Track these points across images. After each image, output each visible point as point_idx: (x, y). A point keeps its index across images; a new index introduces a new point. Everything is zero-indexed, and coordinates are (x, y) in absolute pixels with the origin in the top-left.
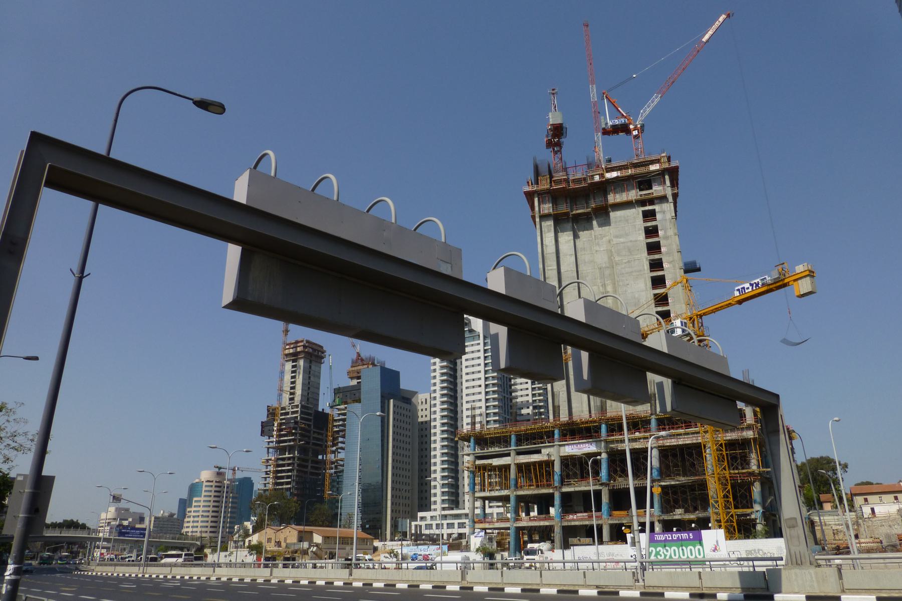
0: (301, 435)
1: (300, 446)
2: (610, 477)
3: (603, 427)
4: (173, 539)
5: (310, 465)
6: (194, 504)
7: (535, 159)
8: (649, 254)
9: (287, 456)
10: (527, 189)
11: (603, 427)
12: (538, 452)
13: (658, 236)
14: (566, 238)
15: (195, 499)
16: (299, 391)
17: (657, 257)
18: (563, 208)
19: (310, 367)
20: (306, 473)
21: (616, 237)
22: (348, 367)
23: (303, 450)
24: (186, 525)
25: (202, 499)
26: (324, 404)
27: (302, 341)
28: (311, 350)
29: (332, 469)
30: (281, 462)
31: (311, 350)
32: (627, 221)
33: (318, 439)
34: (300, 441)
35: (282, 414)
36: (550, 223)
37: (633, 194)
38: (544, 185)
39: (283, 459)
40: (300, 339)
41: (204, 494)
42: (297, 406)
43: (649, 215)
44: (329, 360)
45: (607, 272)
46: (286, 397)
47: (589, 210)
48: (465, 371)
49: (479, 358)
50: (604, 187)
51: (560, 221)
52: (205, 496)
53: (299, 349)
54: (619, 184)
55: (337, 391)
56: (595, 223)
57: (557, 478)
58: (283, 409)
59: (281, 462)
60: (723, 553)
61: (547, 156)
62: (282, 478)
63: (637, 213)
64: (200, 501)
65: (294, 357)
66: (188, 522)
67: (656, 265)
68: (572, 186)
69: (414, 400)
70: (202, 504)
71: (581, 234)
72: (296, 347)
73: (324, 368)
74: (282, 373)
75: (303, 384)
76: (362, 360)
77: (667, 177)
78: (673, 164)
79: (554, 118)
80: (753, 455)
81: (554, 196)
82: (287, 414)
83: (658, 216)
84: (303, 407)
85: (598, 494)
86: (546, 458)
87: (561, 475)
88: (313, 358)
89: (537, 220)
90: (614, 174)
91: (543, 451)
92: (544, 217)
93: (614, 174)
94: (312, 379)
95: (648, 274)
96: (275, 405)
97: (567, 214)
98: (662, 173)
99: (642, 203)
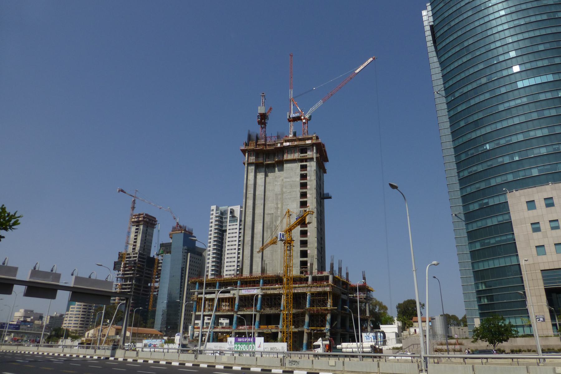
0: (138, 271)
1: (136, 278)
2: (261, 308)
3: (261, 281)
4: (25, 330)
5: (142, 289)
6: (71, 309)
7: (249, 131)
8: (301, 189)
9: (128, 283)
10: (243, 148)
11: (261, 281)
12: (228, 292)
13: (306, 179)
14: (261, 176)
15: (71, 306)
16: (138, 244)
17: (304, 190)
18: (261, 160)
19: (147, 230)
20: (139, 294)
21: (286, 178)
22: (170, 230)
23: (138, 280)
24: (65, 322)
25: (76, 306)
26: (153, 253)
27: (143, 214)
28: (148, 220)
29: (155, 292)
30: (124, 287)
31: (148, 220)
32: (292, 169)
33: (149, 274)
34: (137, 274)
35: (127, 258)
36: (252, 168)
37: (297, 156)
38: (252, 147)
39: (126, 285)
40: (141, 213)
42: (137, 253)
43: (304, 168)
44: (158, 227)
45: (279, 197)
46: (130, 248)
47: (274, 162)
48: (228, 240)
49: (236, 233)
50: (283, 150)
51: (258, 167)
53: (140, 219)
54: (290, 149)
55: (162, 245)
56: (276, 169)
57: (236, 307)
58: (129, 254)
59: (124, 287)
60: (261, 349)
61: (257, 130)
63: (298, 165)
64: (74, 308)
65: (137, 223)
67: (304, 195)
68: (268, 148)
69: (204, 254)
71: (269, 174)
72: (139, 218)
73: (155, 230)
74: (129, 233)
75: (141, 240)
76: (180, 227)
77: (315, 148)
78: (320, 141)
79: (261, 110)
80: (329, 300)
81: (257, 153)
82: (130, 257)
83: (308, 169)
84: (140, 254)
85: (255, 315)
86: (232, 296)
87: (238, 305)
89: (246, 165)
90: (288, 144)
91: (231, 292)
92: (249, 164)
93: (288, 144)
94: (147, 237)
95: (299, 200)
96: (124, 252)
97: (262, 163)
98: (312, 145)
99: (301, 160)
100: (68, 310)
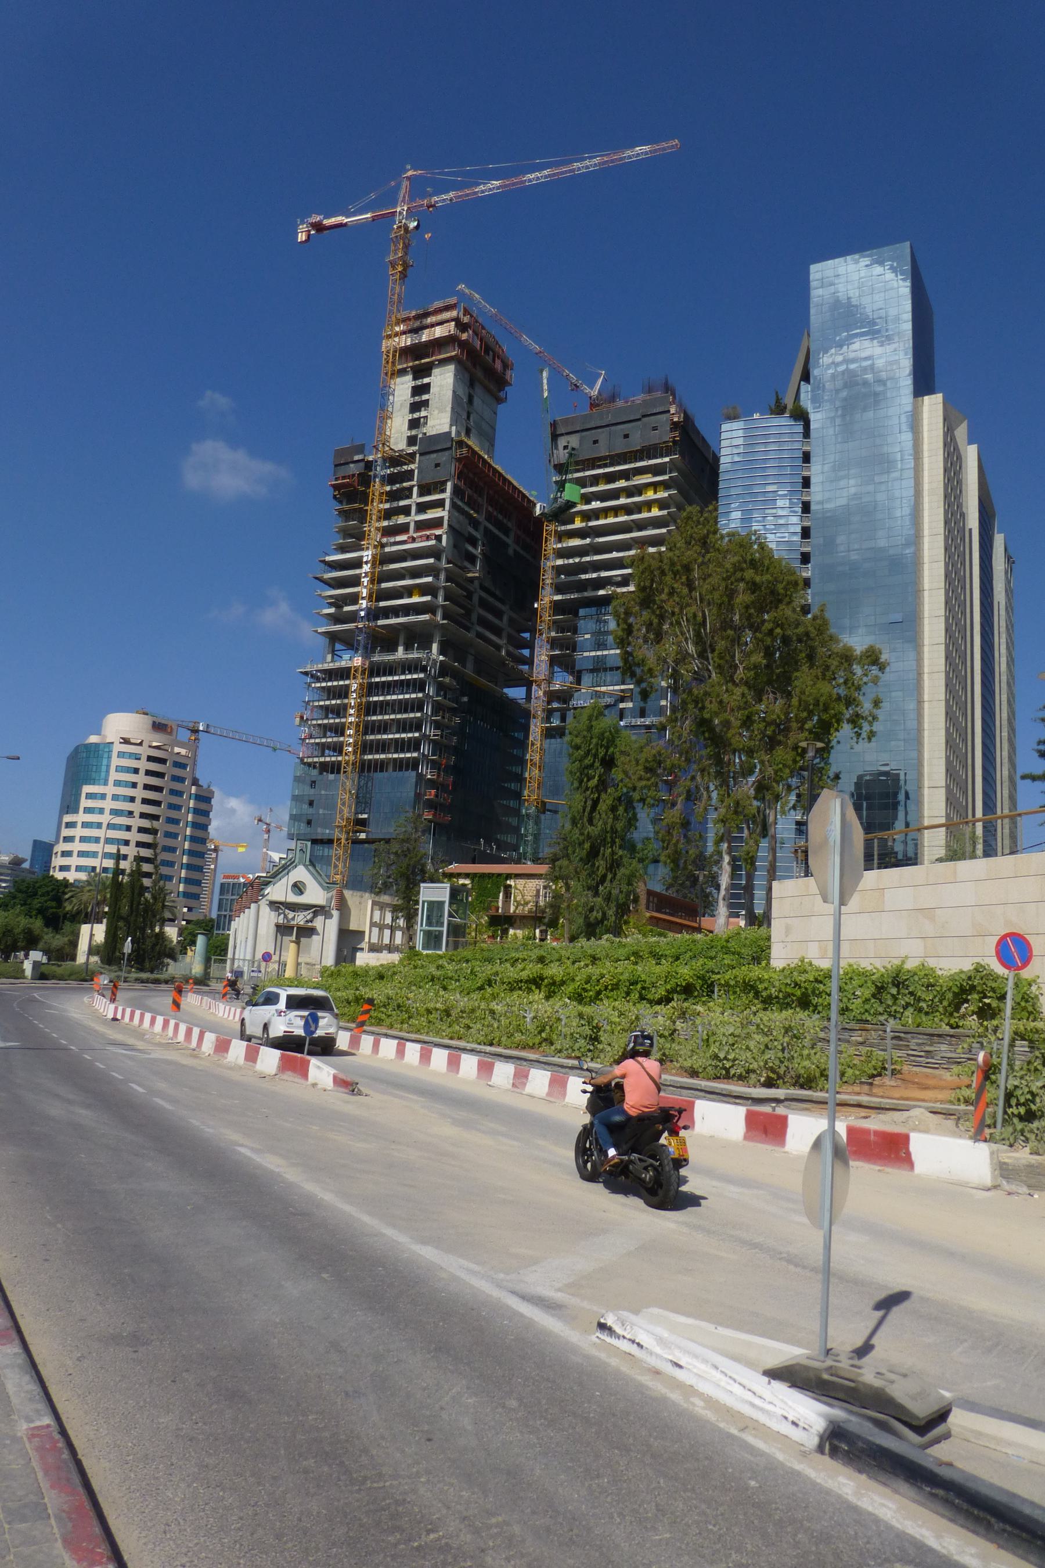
6: (84, 803)
15: (87, 789)
25: (110, 790)
28: (477, 344)
31: (477, 344)
41: (114, 775)
52: (118, 783)
53: (439, 332)
62: (384, 727)
64: (103, 796)
66: (66, 854)
70: (108, 804)
88: (479, 374)
100: (70, 805)
